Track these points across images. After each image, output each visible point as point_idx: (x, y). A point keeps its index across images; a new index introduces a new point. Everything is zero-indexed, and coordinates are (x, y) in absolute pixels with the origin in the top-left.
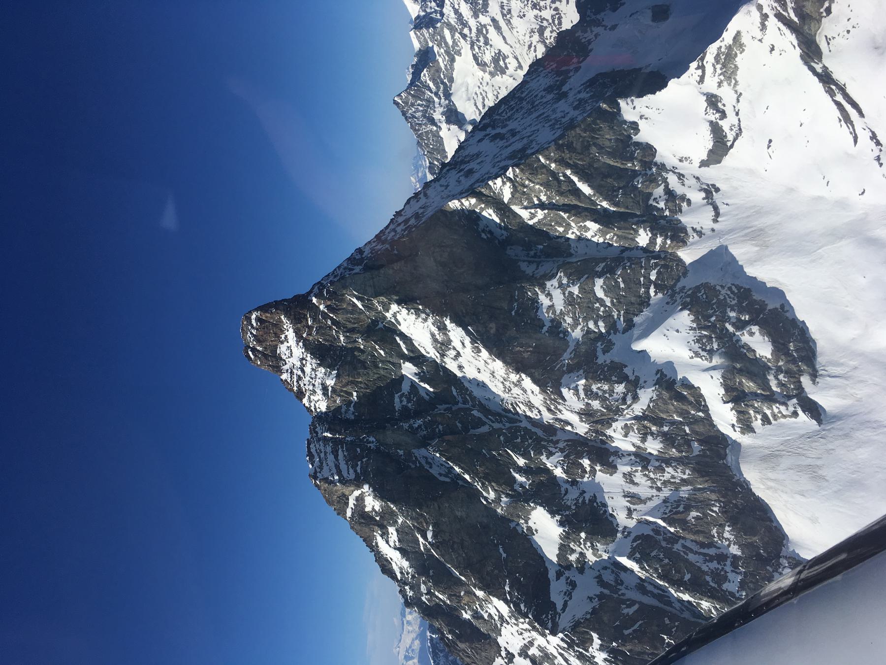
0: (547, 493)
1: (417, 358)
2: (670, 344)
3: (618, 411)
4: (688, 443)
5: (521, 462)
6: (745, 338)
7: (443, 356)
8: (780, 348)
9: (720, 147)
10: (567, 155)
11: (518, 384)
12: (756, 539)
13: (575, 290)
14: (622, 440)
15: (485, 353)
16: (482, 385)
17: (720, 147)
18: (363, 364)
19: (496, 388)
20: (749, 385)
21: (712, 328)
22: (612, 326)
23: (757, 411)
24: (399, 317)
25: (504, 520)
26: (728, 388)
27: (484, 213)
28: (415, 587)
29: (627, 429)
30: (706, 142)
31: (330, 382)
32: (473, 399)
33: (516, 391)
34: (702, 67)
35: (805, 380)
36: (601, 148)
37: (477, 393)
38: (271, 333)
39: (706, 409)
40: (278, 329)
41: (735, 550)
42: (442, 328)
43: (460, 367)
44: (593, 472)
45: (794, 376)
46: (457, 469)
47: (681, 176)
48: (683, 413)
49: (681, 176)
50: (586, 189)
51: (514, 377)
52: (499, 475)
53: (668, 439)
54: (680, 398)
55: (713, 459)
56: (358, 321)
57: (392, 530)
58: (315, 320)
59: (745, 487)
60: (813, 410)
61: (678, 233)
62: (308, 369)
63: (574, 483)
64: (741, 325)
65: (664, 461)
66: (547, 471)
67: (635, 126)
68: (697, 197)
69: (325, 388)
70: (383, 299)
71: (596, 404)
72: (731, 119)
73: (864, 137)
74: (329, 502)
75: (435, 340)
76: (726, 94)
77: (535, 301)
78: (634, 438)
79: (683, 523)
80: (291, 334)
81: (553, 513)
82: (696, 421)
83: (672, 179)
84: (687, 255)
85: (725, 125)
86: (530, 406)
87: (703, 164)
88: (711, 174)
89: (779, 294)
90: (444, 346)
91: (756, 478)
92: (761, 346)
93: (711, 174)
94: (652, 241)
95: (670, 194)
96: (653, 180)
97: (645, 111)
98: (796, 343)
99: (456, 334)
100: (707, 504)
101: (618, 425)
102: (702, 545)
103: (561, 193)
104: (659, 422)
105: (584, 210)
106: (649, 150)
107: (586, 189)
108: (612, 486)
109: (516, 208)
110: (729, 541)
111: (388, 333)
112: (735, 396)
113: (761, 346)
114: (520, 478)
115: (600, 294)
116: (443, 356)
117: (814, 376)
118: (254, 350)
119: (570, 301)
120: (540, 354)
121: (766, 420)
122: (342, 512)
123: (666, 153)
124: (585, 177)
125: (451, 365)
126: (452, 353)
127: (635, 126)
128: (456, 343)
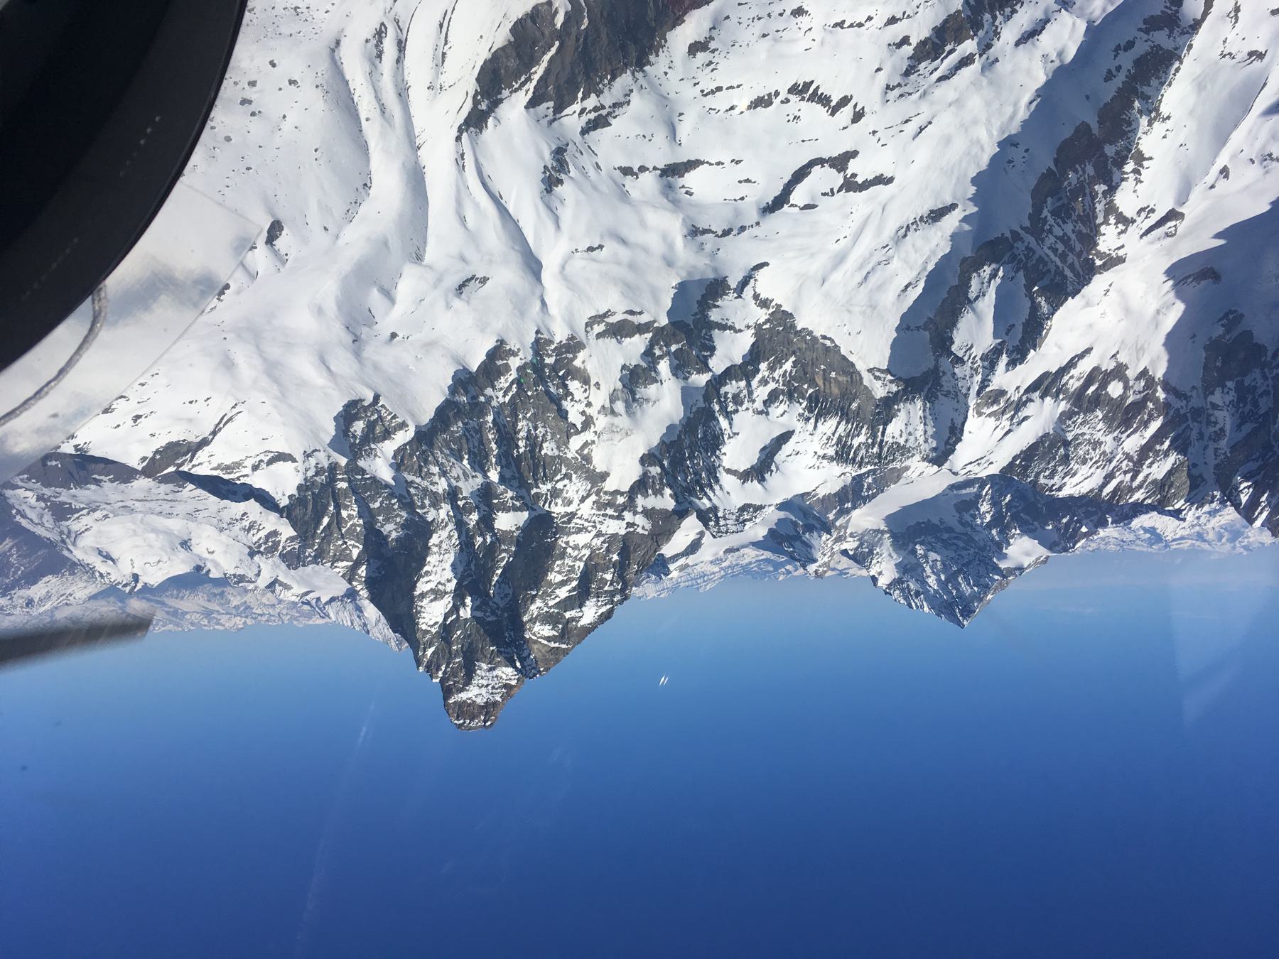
0: (487, 523)
1: (455, 609)
2: (380, 466)
3: (425, 490)
4: (424, 452)
5: (479, 540)
6: (359, 433)
7: (446, 593)
8: (357, 418)
9: (281, 457)
10: (310, 534)
11: (439, 546)
12: (451, 414)
13: (381, 518)
14: (442, 486)
15: (426, 569)
16: (453, 565)
17: (281, 457)
18: (470, 644)
19: (451, 558)
20: (378, 429)
21: (360, 449)
22: (392, 495)
23: (391, 421)
24: (431, 623)
25: (518, 544)
26: (384, 439)
27: (364, 574)
28: (612, 594)
29: (433, 483)
30: (279, 465)
31: (484, 666)
32: (465, 571)
33: (444, 546)
34: (238, 478)
35: (366, 404)
36: (305, 514)
37: (461, 569)
38: (466, 710)
39: (405, 445)
40: (462, 704)
41: (460, 424)
42: (423, 596)
43: (449, 581)
44: (465, 498)
45: (366, 409)
46: (496, 578)
47: (307, 470)
48: (411, 456)
49: (307, 470)
50: (326, 520)
51: (435, 549)
52: (491, 550)
53: (426, 462)
54: (402, 460)
55: (425, 437)
56: (443, 650)
57: (568, 615)
58: (448, 680)
59: (432, 420)
60: (377, 398)
61: (333, 468)
62: (485, 682)
63: (477, 507)
64: (354, 437)
65: (437, 463)
66: (478, 523)
67: (290, 497)
68: (312, 461)
69: (490, 670)
70: (419, 635)
71: (427, 502)
72: (261, 457)
73: (235, 411)
74: (557, 661)
75: (435, 599)
76: (249, 463)
77: (398, 540)
78: (436, 479)
79: (460, 451)
80: (463, 696)
81: (494, 520)
82: (411, 449)
83: (310, 474)
84: (343, 461)
85: (266, 459)
86: (450, 537)
87: (294, 460)
88: (299, 456)
89: (335, 418)
90: (437, 594)
91: (427, 416)
92: (359, 427)
93: (299, 456)
94: (342, 480)
95: (317, 474)
96: (313, 483)
97: (280, 494)
98: (350, 412)
99: (422, 587)
100: (445, 440)
101: (434, 488)
102: (468, 440)
103: (331, 534)
104: (420, 467)
105: (338, 520)
106: (300, 488)
107: (326, 520)
108: (468, 487)
109: (355, 557)
110: (457, 428)
111: (446, 630)
112: (387, 434)
113: (359, 427)
114: (489, 540)
115: (377, 505)
116: (446, 593)
117: (362, 400)
118: (485, 721)
119: (387, 520)
120: (419, 532)
121: (395, 417)
122: (566, 652)
123: (299, 479)
124: (319, 522)
125: (451, 586)
126: (440, 587)
127: (290, 497)
128: (432, 585)
